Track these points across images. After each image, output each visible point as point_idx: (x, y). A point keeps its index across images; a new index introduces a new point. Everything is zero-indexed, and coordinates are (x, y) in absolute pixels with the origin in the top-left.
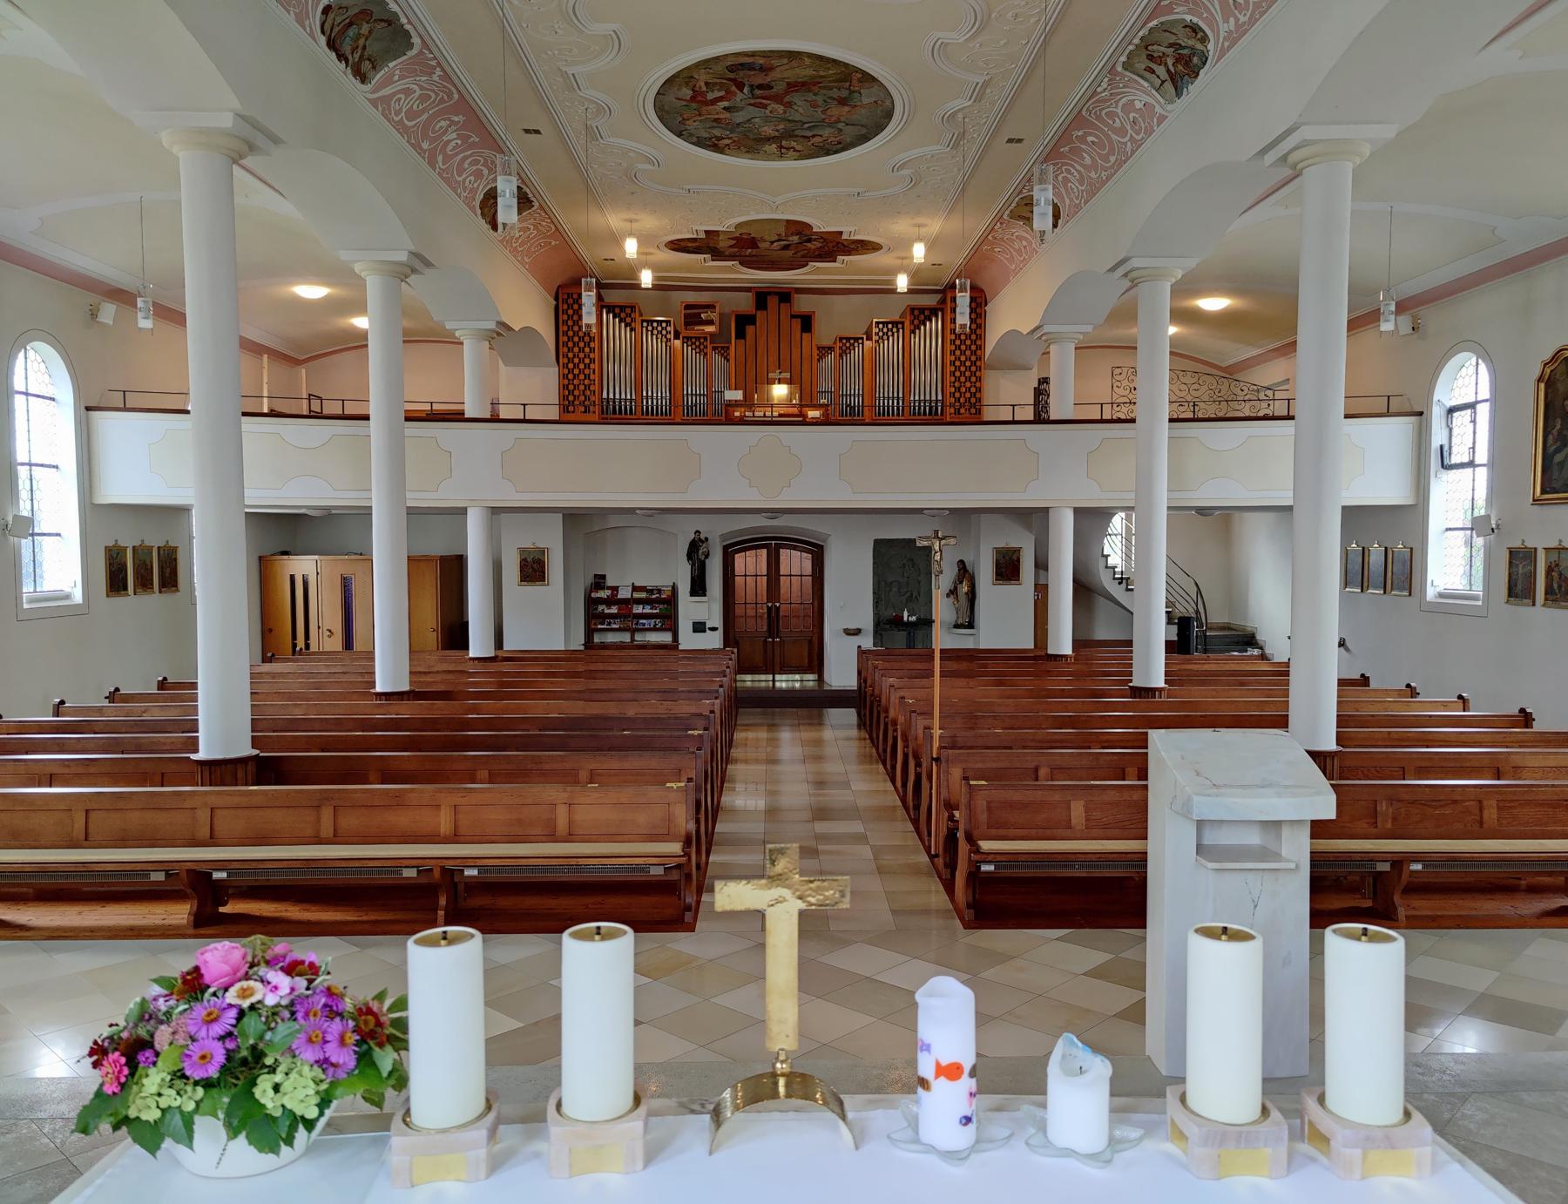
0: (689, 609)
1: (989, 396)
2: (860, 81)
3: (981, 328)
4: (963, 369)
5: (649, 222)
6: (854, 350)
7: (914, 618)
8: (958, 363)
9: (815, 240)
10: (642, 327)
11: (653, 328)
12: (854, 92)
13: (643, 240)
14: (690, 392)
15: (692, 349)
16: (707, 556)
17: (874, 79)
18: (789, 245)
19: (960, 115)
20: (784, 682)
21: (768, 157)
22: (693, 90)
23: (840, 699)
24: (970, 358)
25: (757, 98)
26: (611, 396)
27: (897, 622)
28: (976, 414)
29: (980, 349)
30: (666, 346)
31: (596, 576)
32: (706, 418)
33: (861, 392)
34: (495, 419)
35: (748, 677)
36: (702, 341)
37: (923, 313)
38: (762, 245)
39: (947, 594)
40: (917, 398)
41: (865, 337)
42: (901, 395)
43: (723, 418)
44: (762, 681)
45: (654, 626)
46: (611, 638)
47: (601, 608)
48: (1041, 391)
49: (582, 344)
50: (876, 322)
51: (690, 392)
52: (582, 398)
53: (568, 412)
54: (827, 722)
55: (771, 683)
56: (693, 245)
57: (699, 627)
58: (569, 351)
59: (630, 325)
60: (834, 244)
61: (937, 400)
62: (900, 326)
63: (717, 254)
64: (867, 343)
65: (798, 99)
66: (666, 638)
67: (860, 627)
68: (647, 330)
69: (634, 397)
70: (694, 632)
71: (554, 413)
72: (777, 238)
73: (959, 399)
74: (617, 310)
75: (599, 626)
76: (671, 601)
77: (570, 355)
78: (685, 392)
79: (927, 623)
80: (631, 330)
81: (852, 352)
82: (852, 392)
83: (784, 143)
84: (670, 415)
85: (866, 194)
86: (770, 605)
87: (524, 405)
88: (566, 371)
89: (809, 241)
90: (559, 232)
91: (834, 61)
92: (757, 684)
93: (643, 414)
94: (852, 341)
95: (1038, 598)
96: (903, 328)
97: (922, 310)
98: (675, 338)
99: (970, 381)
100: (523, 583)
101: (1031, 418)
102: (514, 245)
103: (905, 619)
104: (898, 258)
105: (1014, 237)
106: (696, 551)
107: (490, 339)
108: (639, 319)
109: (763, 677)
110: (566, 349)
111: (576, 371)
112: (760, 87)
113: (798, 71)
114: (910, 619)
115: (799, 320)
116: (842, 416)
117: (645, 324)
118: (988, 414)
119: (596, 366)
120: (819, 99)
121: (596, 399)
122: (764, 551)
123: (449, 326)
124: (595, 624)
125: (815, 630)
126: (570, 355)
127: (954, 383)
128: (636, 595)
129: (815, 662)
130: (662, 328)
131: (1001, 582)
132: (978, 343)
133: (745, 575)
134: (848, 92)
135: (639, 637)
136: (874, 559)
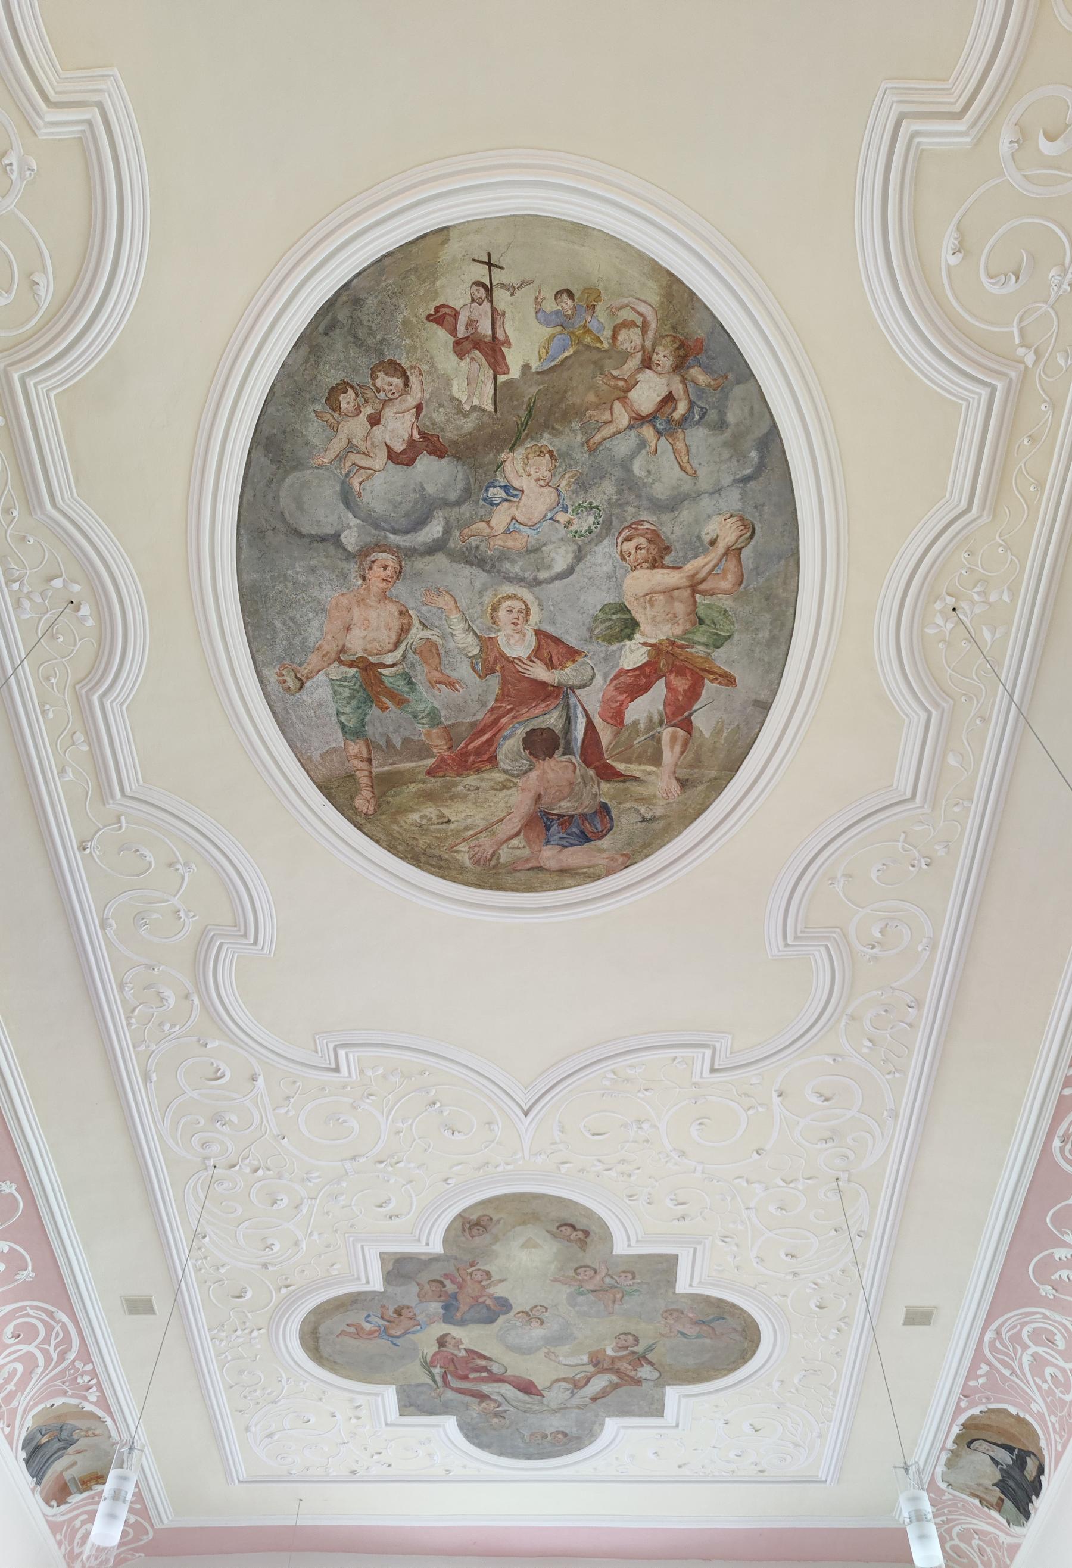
17: (326, 789)
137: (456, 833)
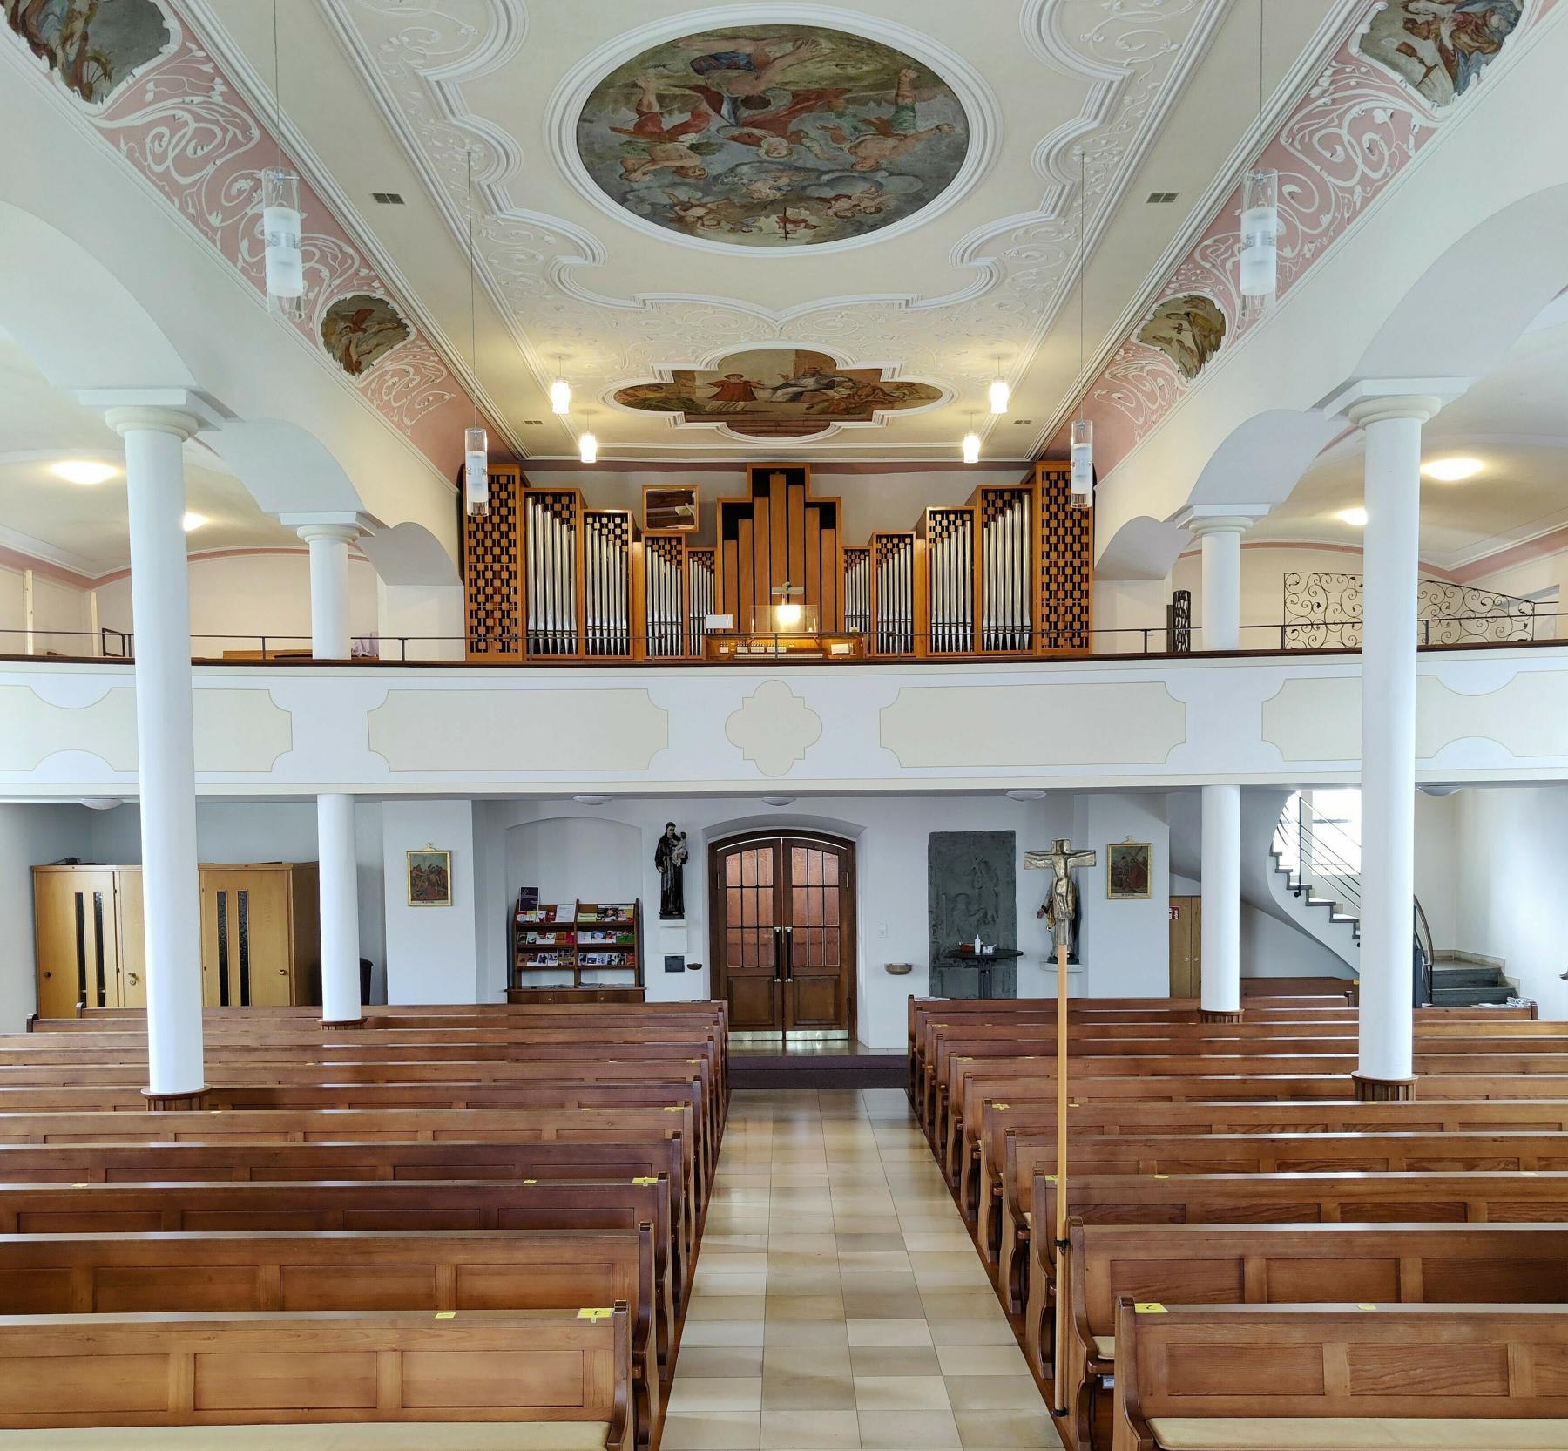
0: (660, 938)
1: (1098, 619)
2: (915, 85)
3: (1087, 518)
4: (1061, 579)
5: (588, 358)
6: (899, 553)
7: (989, 950)
8: (1053, 571)
9: (841, 384)
10: (586, 523)
11: (602, 526)
12: (905, 108)
13: (583, 388)
14: (656, 619)
15: (659, 556)
16: (684, 861)
17: (937, 81)
18: (801, 394)
19: (1077, 150)
20: (800, 1041)
21: (766, 239)
22: (639, 112)
23: (880, 1072)
24: (1072, 563)
25: (745, 125)
26: (541, 626)
27: (965, 955)
28: (1081, 646)
29: (1087, 549)
30: (621, 552)
31: (523, 889)
32: (680, 657)
33: (909, 617)
34: (363, 661)
35: (747, 1035)
36: (674, 543)
37: (1002, 498)
38: (761, 394)
39: (1039, 913)
40: (993, 623)
41: (914, 534)
42: (969, 620)
43: (703, 656)
44: (764, 1041)
45: (609, 962)
46: (547, 980)
47: (531, 936)
48: (1180, 611)
49: (497, 551)
50: (931, 512)
51: (656, 619)
52: (498, 630)
53: (478, 651)
54: (863, 1114)
55: (780, 1043)
56: (657, 395)
57: (674, 964)
58: (478, 561)
59: (568, 522)
60: (868, 390)
61: (1022, 627)
62: (967, 517)
63: (694, 411)
64: (919, 545)
65: (809, 124)
66: (625, 979)
67: (909, 962)
68: (593, 528)
69: (574, 628)
70: (667, 970)
71: (458, 651)
72: (782, 381)
73: (1056, 624)
74: (549, 500)
75: (530, 964)
76: (633, 926)
77: (481, 567)
78: (650, 620)
79: (1008, 955)
80: (571, 528)
81: (896, 556)
82: (897, 617)
83: (789, 212)
84: (628, 654)
85: (920, 303)
86: (778, 929)
87: (403, 639)
88: (474, 591)
89: (831, 385)
90: (453, 379)
91: (872, 46)
92: (759, 1046)
93: (587, 653)
94: (896, 541)
95: (1173, 918)
96: (971, 520)
97: (999, 493)
98: (634, 540)
99: (1071, 596)
100: (415, 903)
101: (1163, 649)
102: (386, 398)
103: (977, 950)
104: (965, 412)
105: (1145, 374)
106: (668, 851)
107: (352, 542)
108: (580, 513)
109: (768, 1035)
110: (474, 559)
111: (489, 591)
112: (748, 102)
113: (810, 66)
114: (985, 950)
115: (817, 510)
116: (882, 651)
117: (590, 520)
118: (1100, 644)
119: (517, 582)
120: (846, 124)
121: (518, 630)
122: (770, 851)
123: (286, 520)
124: (523, 960)
125: (845, 966)
126: (481, 567)
127: (1048, 600)
128: (583, 918)
129: (844, 1013)
130: (616, 526)
131: (1119, 895)
132: (1084, 539)
133: (742, 887)
134: (893, 109)
135: (586, 978)
136: (930, 862)
137: (833, 59)
